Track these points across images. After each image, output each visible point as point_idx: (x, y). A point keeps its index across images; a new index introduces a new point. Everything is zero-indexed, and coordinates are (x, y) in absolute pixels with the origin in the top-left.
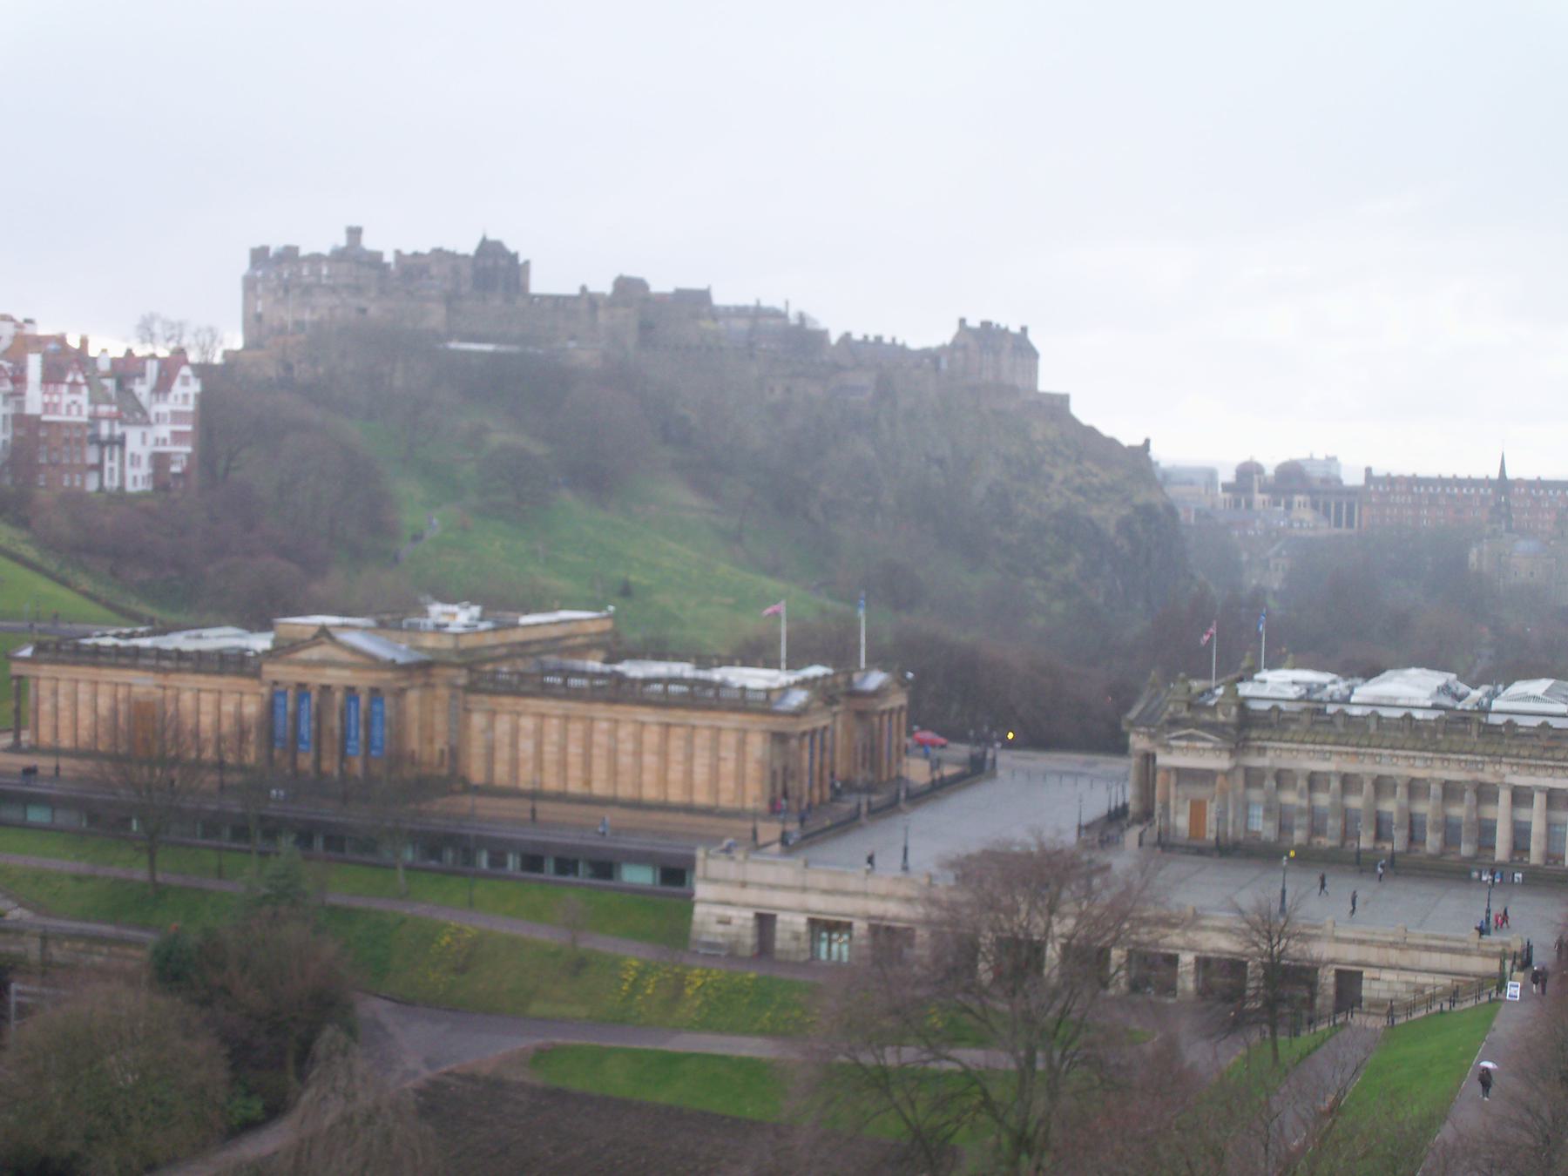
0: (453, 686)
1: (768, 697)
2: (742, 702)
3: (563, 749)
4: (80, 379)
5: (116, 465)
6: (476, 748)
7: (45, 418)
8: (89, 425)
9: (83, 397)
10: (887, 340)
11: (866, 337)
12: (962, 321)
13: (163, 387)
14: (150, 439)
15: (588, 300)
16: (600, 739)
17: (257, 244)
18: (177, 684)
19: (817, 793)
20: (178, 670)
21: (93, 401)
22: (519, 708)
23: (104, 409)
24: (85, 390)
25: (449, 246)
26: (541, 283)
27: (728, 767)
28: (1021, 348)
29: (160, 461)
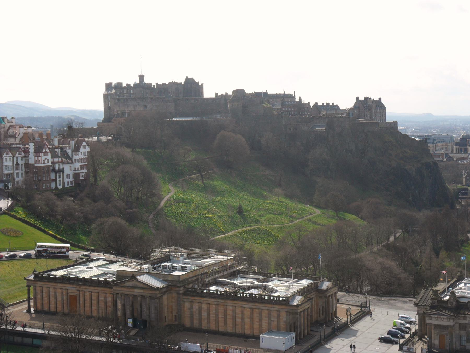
0: (178, 293)
4: (48, 150)
5: (61, 179)
6: (187, 314)
7: (36, 165)
8: (51, 166)
9: (49, 157)
10: (331, 104)
11: (323, 104)
12: (357, 98)
13: (77, 149)
14: (73, 169)
16: (229, 312)
18: (83, 290)
19: (306, 331)
20: (84, 285)
21: (52, 157)
22: (202, 301)
23: (56, 160)
24: (49, 154)
25: (175, 80)
26: (209, 93)
28: (378, 106)
29: (76, 176)
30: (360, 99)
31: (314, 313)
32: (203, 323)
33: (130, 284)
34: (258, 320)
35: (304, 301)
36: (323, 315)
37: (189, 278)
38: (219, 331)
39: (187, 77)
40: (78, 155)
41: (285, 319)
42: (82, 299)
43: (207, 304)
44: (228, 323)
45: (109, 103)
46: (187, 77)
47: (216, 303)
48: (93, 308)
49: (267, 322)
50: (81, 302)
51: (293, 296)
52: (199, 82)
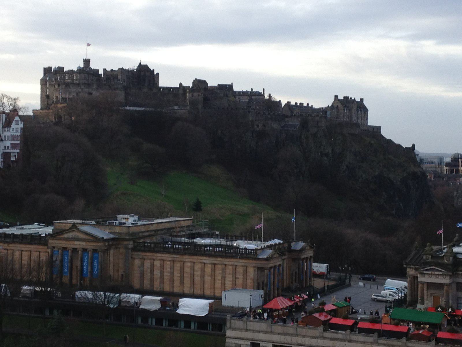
0: (126, 248)
1: (256, 253)
2: (247, 254)
3: (172, 274)
6: (136, 274)
10: (305, 105)
11: (296, 103)
12: (336, 97)
16: (187, 270)
17: (47, 67)
18: (12, 248)
20: (13, 242)
22: (154, 257)
26: (163, 82)
28: (360, 107)
30: (339, 98)
32: (155, 283)
34: (220, 278)
35: (275, 256)
36: (295, 282)
37: (140, 232)
38: (173, 292)
39: (140, 63)
40: (9, 131)
43: (160, 260)
44: (185, 282)
45: (48, 90)
46: (140, 63)
49: (231, 279)
51: (262, 249)
52: (154, 70)
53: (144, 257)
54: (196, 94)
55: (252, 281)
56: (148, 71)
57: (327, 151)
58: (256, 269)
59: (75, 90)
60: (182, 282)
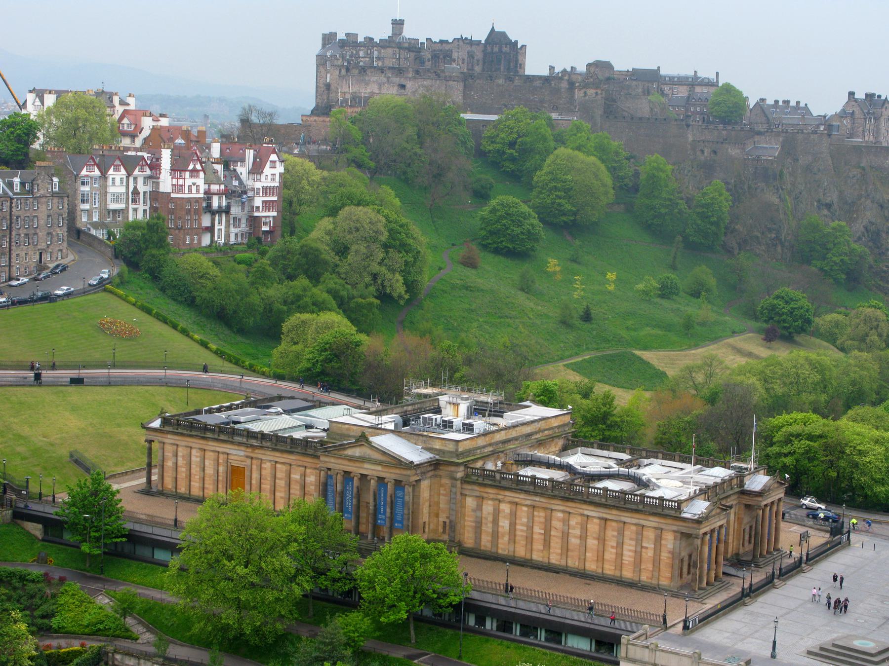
1: (679, 507)
4: (198, 167)
5: (223, 227)
6: (469, 522)
7: (173, 195)
8: (204, 199)
9: (200, 181)
11: (777, 102)
12: (851, 94)
13: (257, 169)
15: (569, 76)
16: (556, 523)
19: (713, 574)
21: (208, 182)
22: (500, 497)
23: (215, 188)
24: (202, 174)
27: (649, 554)
30: (856, 96)
31: (731, 537)
32: (500, 541)
33: (357, 452)
34: (615, 545)
35: (714, 513)
36: (750, 542)
38: (531, 559)
41: (670, 546)
42: (255, 475)
43: (510, 503)
45: (329, 75)
47: (528, 503)
48: (278, 494)
49: (633, 548)
50: (254, 482)
51: (691, 499)
52: (516, 42)
53: (485, 495)
54: (591, 92)
55: (670, 556)
56: (506, 44)
57: (828, 200)
58: (679, 535)
59: (374, 79)
60: (547, 544)
